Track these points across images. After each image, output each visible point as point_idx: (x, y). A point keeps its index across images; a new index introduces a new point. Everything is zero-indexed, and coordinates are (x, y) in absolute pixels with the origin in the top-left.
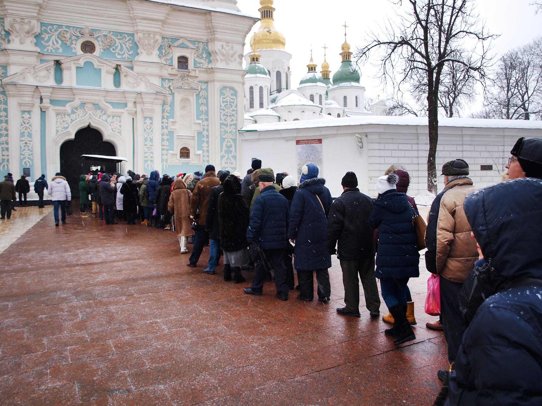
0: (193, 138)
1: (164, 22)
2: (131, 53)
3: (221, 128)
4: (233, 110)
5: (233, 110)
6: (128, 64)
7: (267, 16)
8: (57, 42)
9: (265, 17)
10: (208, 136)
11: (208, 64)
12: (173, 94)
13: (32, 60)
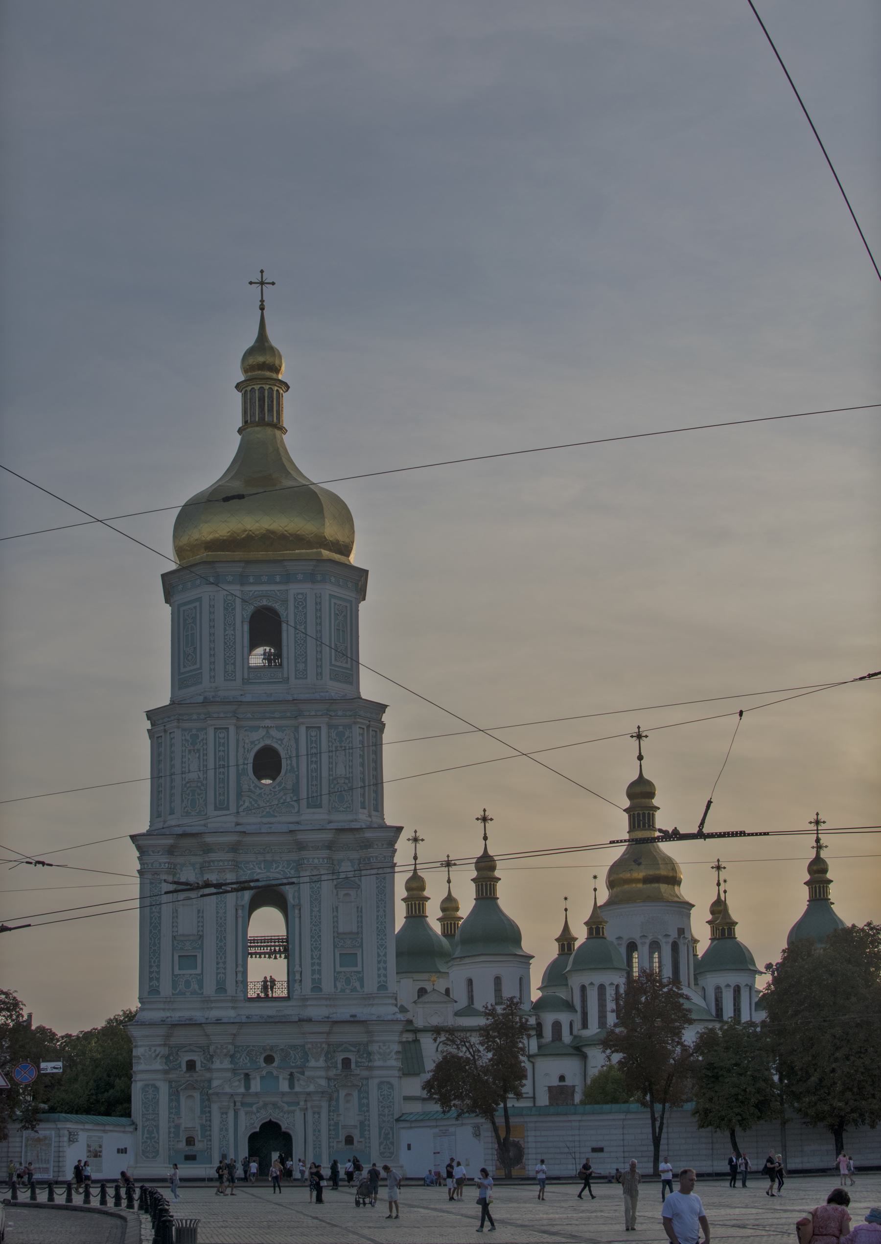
0: (355, 1127)
1: (328, 1033)
2: (302, 1061)
3: (379, 1118)
4: (390, 1102)
5: (390, 1102)
6: (300, 1070)
7: (639, 826)
8: (246, 1058)
9: (634, 827)
10: (369, 1126)
11: (369, 1062)
12: (338, 1091)
13: (229, 1075)
